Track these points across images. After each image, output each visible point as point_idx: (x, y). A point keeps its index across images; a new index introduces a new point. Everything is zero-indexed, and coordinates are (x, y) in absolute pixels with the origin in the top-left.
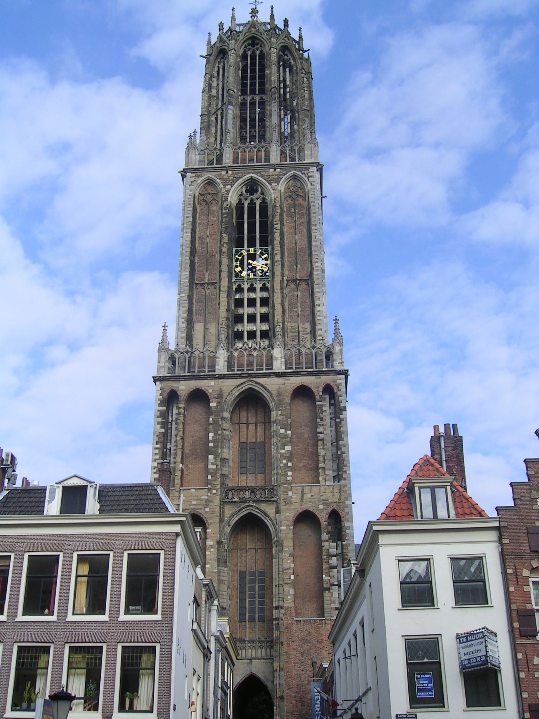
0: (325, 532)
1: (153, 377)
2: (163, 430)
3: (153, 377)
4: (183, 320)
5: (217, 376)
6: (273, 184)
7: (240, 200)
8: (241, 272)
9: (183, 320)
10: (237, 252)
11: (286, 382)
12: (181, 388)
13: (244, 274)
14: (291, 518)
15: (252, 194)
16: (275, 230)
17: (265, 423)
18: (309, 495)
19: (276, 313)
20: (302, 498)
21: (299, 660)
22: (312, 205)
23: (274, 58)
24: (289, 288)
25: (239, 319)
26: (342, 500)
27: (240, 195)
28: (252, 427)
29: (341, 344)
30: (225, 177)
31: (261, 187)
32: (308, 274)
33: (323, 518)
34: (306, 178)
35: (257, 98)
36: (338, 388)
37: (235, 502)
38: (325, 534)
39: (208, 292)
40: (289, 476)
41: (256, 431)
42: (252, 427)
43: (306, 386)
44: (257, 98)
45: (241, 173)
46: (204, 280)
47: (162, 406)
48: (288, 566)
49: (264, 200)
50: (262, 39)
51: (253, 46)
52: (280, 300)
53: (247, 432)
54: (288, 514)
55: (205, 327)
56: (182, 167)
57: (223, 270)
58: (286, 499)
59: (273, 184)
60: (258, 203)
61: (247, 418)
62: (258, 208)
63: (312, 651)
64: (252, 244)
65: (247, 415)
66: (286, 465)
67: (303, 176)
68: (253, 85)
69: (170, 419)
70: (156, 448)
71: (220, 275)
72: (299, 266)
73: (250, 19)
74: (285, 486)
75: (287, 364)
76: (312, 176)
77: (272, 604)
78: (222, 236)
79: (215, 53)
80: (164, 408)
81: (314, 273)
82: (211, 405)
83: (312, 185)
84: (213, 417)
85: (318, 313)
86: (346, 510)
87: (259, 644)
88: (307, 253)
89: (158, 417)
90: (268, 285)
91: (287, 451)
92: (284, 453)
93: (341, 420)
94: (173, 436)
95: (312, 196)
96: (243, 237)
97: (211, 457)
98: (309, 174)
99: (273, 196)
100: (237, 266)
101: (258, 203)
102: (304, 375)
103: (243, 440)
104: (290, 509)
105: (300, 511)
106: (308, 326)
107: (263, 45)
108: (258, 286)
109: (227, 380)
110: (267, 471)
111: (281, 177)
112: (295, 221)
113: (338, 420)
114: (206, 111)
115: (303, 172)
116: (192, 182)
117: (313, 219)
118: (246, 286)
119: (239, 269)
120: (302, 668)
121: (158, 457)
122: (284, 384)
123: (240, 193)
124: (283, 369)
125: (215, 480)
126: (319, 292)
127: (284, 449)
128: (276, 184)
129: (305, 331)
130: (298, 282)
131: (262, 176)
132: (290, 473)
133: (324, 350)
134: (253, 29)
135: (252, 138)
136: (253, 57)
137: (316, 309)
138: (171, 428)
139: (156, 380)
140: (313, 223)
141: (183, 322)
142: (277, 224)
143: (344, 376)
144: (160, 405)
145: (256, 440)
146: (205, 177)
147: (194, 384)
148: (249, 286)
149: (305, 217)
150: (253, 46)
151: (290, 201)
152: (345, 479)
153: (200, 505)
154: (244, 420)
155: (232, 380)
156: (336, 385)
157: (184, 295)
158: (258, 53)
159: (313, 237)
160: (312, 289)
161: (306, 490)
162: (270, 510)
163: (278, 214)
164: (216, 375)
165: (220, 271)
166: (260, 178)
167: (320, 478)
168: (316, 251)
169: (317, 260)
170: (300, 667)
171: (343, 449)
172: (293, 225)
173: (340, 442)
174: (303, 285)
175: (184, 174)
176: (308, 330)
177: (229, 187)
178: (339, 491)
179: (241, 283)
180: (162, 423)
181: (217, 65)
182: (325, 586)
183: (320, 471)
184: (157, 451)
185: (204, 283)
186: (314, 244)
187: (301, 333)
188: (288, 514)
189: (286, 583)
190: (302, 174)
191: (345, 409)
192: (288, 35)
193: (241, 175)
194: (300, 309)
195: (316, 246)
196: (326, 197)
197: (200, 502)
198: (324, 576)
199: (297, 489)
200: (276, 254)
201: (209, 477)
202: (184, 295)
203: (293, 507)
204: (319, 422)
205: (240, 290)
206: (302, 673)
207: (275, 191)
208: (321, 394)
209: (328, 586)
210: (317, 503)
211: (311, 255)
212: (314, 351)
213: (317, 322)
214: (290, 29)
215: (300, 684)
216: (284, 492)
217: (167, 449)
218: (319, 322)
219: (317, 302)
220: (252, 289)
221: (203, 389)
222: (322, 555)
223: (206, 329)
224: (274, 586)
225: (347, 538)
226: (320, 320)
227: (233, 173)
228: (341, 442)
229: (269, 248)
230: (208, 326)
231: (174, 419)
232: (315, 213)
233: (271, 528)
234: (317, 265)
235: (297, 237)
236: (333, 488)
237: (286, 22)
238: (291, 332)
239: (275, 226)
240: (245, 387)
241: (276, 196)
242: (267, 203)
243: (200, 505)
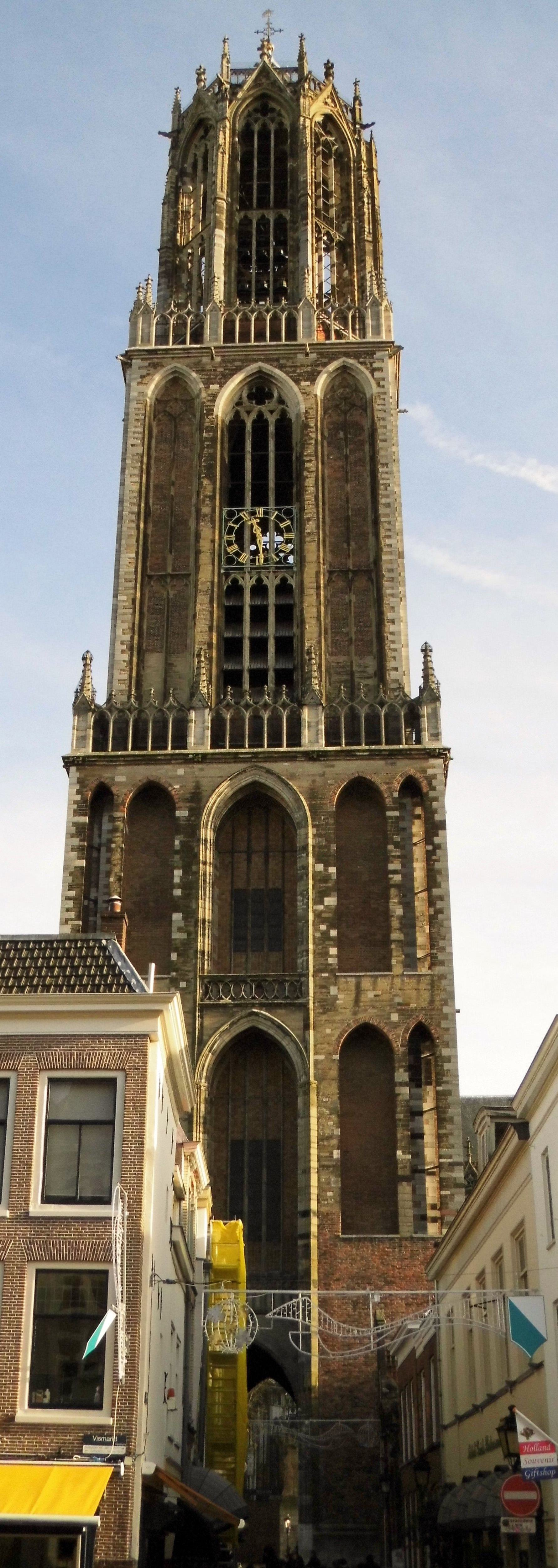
0: (402, 1067)
1: (64, 758)
2: (83, 863)
3: (64, 758)
4: (124, 647)
5: (191, 756)
6: (303, 383)
7: (237, 414)
8: (238, 554)
9: (124, 647)
10: (231, 514)
11: (327, 770)
12: (118, 779)
13: (245, 558)
14: (334, 1039)
15: (260, 402)
16: (305, 473)
18: (371, 995)
19: (307, 636)
20: (357, 1001)
22: (380, 424)
24: (334, 588)
26: (437, 1003)
27: (239, 403)
28: (258, 860)
29: (435, 698)
30: (209, 367)
31: (278, 388)
32: (372, 559)
33: (398, 1040)
34: (367, 373)
35: (271, 216)
36: (430, 784)
37: (225, 1006)
38: (402, 1070)
39: (172, 593)
40: (332, 956)
41: (267, 869)
42: (258, 860)
43: (365, 779)
44: (271, 216)
45: (240, 360)
46: (165, 569)
47: (81, 815)
48: (328, 1132)
49: (284, 413)
50: (282, 101)
52: (315, 610)
53: (248, 868)
54: (328, 1031)
55: (166, 659)
57: (202, 549)
58: (325, 1000)
59: (303, 383)
60: (272, 419)
61: (249, 841)
62: (272, 429)
64: (260, 499)
65: (249, 834)
66: (325, 935)
67: (362, 368)
68: (263, 189)
69: (96, 841)
70: (68, 898)
71: (197, 560)
72: (353, 544)
73: (259, 60)
74: (323, 975)
76: (380, 369)
77: (296, 1207)
78: (200, 484)
79: (188, 126)
80: (86, 819)
81: (384, 557)
82: (178, 813)
83: (378, 385)
84: (182, 837)
85: (391, 638)
86: (444, 1024)
89: (72, 836)
90: (292, 582)
91: (327, 907)
92: (322, 912)
93: (437, 847)
94: (102, 876)
95: (380, 407)
96: (243, 486)
97: (177, 917)
98: (375, 365)
99: (303, 407)
100: (230, 543)
101: (272, 419)
102: (362, 758)
103: (240, 884)
104: (334, 1022)
106: (371, 664)
107: (283, 112)
108: (271, 582)
109: (211, 766)
110: (287, 947)
111: (319, 369)
112: (346, 457)
113: (430, 848)
114: (169, 240)
115: (361, 360)
116: (143, 377)
117: (382, 453)
118: (248, 583)
121: (72, 915)
122: (323, 775)
123: (236, 400)
124: (321, 745)
125: (185, 962)
126: (393, 595)
127: (322, 903)
128: (308, 383)
129: (364, 672)
130: (350, 575)
131: (281, 367)
132: (333, 951)
134: (264, 80)
135: (262, 294)
136: (264, 135)
137: (386, 629)
138: (98, 860)
139: (69, 762)
140: (382, 461)
141: (123, 651)
142: (310, 461)
143: (441, 761)
144: (77, 813)
145: (267, 883)
146: (169, 367)
147: (144, 773)
148: (253, 581)
149: (367, 447)
151: (335, 418)
152: (442, 963)
154: (243, 846)
155: (220, 766)
156: (426, 778)
157: (125, 598)
158: (272, 127)
159: (382, 487)
160: (379, 589)
161: (366, 983)
163: (313, 441)
164: (187, 755)
165: (198, 552)
166: (277, 372)
167: (394, 961)
168: (387, 515)
169: (388, 533)
171: (439, 904)
172: (340, 463)
173: (434, 890)
174: (361, 583)
176: (371, 670)
177: (214, 387)
178: (429, 987)
179: (239, 577)
180: (80, 849)
181: (192, 151)
182: (400, 1173)
183: (393, 946)
184: (71, 904)
185: (166, 576)
186: (383, 501)
187: (357, 675)
190: (361, 363)
191: (442, 825)
192: (334, 95)
193: (237, 364)
194: (354, 629)
195: (388, 505)
196: (405, 411)
198: (399, 1153)
199: (347, 982)
200: (309, 519)
201: (174, 956)
202: (125, 598)
203: (338, 1018)
204: (392, 851)
205: (235, 590)
207: (307, 397)
208: (396, 795)
209: (407, 1172)
211: (376, 523)
213: (389, 654)
216: (322, 987)
217: (89, 900)
218: (394, 654)
219: (389, 615)
220: (259, 590)
221: (162, 781)
222: (394, 1112)
223: (168, 667)
224: (299, 1172)
225: (445, 1079)
226: (395, 650)
227: (223, 361)
228: (435, 891)
229: (294, 508)
230: (173, 659)
231: (104, 840)
232: (385, 441)
233: (295, 1058)
234: (388, 541)
235: (348, 488)
236: (419, 982)
237: (329, 68)
238: (339, 673)
239: (307, 465)
240: (245, 780)
241: (309, 405)
242: (290, 420)
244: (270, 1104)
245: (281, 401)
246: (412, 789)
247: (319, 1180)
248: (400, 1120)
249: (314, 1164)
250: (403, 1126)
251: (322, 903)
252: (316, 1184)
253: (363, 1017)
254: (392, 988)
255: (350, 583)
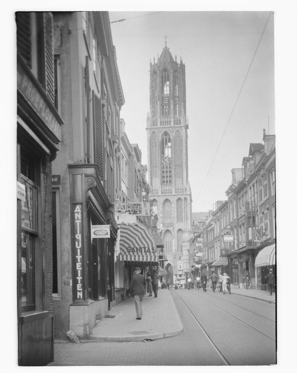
10: (163, 156)
23: (172, 78)
25: (164, 177)
51: (165, 72)
56: (146, 127)
60: (168, 138)
75: (176, 192)
83: (183, 134)
90: (171, 167)
101: (168, 138)
108: (168, 167)
119: (163, 162)
133: (184, 188)
150: (165, 72)
158: (166, 75)
175: (147, 129)
181: (154, 76)
188: (176, 230)
205: (163, 168)
212: (182, 188)
214: (177, 61)
220: (167, 168)
245: (169, 136)
246: (185, 199)
255: (179, 167)
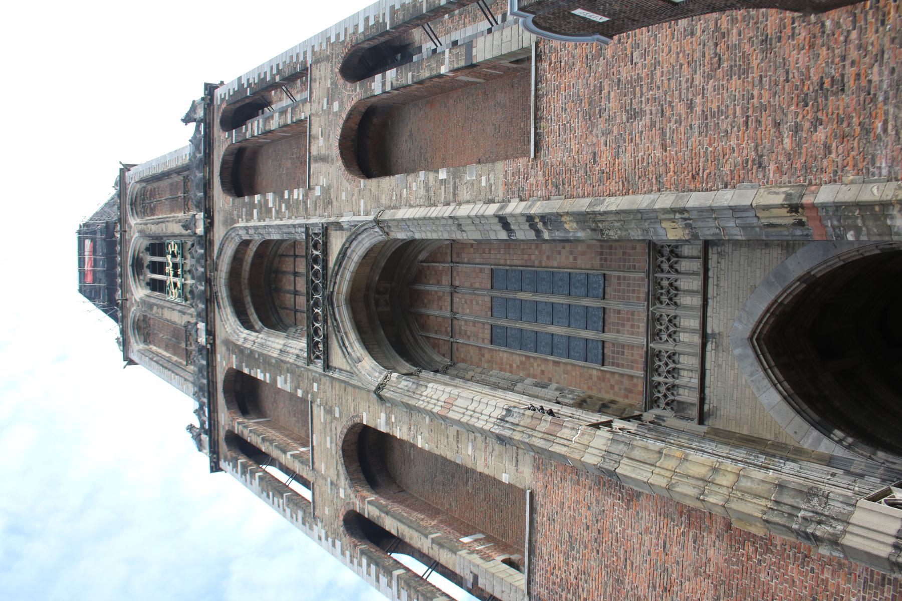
0: (371, 86)
5: (209, 346)
7: (148, 284)
17: (296, 256)
21: (653, 124)
48: (422, 192)
63: (624, 75)
87: (664, 298)
88: (170, 181)
105: (340, 163)
120: (681, 108)
127: (271, 208)
153: (331, 430)
162: (337, 243)
170: (679, 122)
189: (454, 195)
197: (328, 429)
198: (443, 70)
206: (698, 109)
210: (331, 117)
215: (745, 110)
243: (331, 430)
244: (457, 283)
247: (468, 202)
248: (413, 76)
249: (447, 211)
250: (418, 72)
251: (271, 208)
252: (471, 206)
253: (335, 151)
254: (317, 115)
